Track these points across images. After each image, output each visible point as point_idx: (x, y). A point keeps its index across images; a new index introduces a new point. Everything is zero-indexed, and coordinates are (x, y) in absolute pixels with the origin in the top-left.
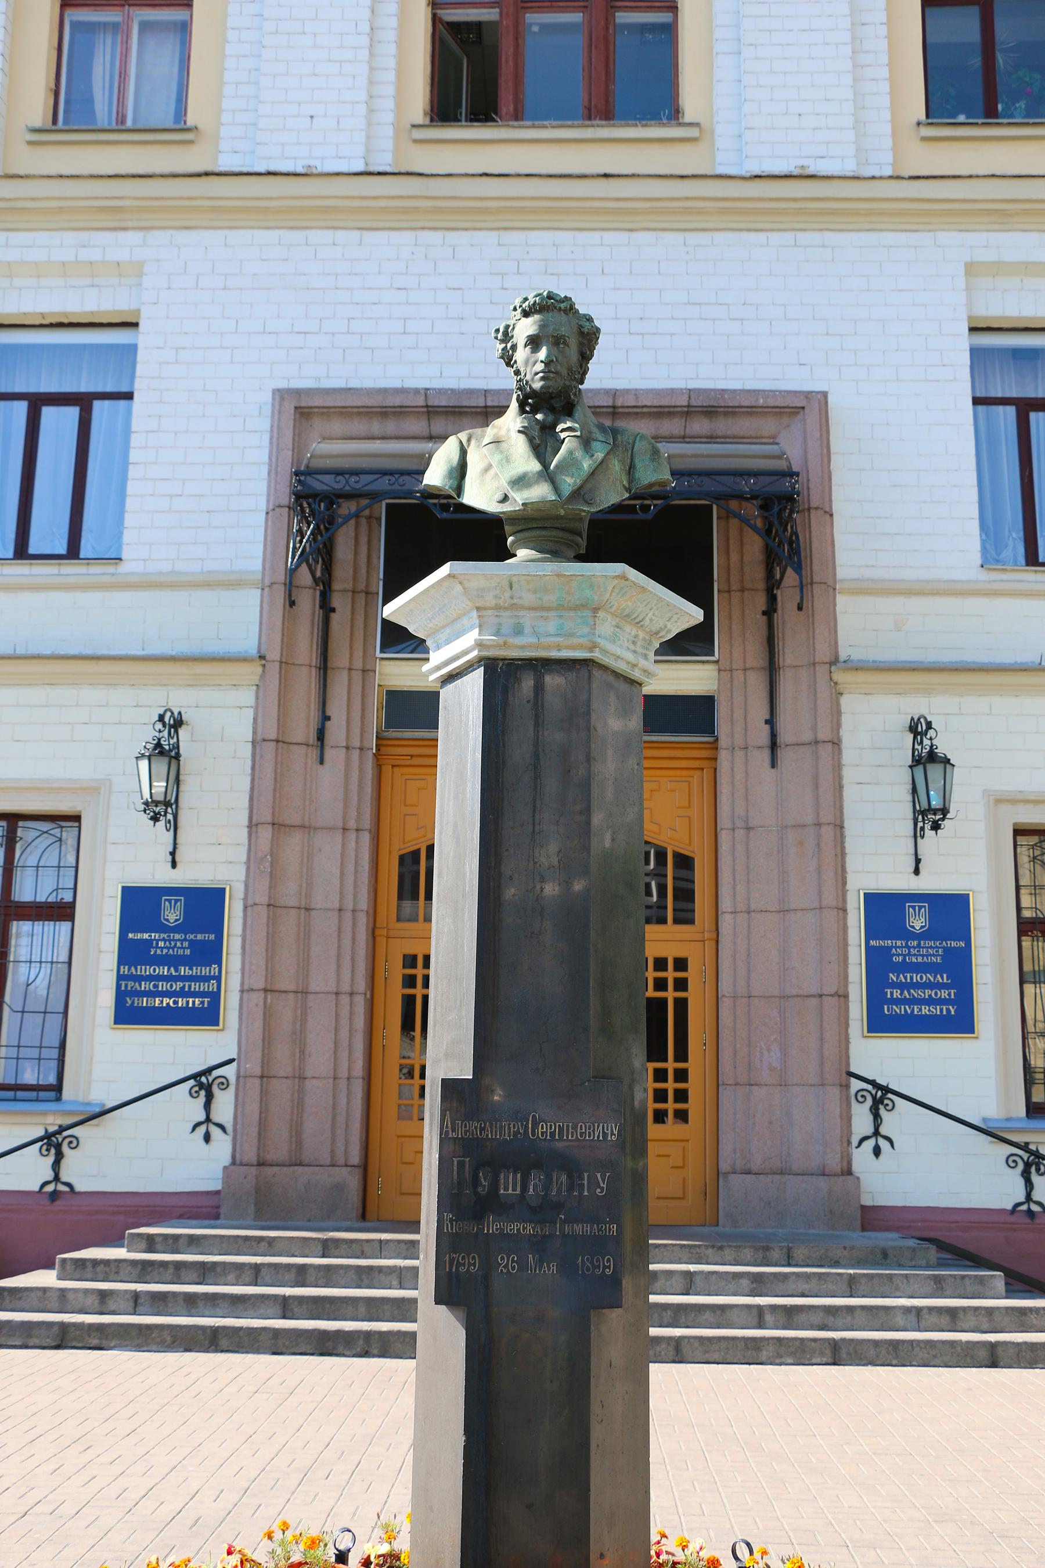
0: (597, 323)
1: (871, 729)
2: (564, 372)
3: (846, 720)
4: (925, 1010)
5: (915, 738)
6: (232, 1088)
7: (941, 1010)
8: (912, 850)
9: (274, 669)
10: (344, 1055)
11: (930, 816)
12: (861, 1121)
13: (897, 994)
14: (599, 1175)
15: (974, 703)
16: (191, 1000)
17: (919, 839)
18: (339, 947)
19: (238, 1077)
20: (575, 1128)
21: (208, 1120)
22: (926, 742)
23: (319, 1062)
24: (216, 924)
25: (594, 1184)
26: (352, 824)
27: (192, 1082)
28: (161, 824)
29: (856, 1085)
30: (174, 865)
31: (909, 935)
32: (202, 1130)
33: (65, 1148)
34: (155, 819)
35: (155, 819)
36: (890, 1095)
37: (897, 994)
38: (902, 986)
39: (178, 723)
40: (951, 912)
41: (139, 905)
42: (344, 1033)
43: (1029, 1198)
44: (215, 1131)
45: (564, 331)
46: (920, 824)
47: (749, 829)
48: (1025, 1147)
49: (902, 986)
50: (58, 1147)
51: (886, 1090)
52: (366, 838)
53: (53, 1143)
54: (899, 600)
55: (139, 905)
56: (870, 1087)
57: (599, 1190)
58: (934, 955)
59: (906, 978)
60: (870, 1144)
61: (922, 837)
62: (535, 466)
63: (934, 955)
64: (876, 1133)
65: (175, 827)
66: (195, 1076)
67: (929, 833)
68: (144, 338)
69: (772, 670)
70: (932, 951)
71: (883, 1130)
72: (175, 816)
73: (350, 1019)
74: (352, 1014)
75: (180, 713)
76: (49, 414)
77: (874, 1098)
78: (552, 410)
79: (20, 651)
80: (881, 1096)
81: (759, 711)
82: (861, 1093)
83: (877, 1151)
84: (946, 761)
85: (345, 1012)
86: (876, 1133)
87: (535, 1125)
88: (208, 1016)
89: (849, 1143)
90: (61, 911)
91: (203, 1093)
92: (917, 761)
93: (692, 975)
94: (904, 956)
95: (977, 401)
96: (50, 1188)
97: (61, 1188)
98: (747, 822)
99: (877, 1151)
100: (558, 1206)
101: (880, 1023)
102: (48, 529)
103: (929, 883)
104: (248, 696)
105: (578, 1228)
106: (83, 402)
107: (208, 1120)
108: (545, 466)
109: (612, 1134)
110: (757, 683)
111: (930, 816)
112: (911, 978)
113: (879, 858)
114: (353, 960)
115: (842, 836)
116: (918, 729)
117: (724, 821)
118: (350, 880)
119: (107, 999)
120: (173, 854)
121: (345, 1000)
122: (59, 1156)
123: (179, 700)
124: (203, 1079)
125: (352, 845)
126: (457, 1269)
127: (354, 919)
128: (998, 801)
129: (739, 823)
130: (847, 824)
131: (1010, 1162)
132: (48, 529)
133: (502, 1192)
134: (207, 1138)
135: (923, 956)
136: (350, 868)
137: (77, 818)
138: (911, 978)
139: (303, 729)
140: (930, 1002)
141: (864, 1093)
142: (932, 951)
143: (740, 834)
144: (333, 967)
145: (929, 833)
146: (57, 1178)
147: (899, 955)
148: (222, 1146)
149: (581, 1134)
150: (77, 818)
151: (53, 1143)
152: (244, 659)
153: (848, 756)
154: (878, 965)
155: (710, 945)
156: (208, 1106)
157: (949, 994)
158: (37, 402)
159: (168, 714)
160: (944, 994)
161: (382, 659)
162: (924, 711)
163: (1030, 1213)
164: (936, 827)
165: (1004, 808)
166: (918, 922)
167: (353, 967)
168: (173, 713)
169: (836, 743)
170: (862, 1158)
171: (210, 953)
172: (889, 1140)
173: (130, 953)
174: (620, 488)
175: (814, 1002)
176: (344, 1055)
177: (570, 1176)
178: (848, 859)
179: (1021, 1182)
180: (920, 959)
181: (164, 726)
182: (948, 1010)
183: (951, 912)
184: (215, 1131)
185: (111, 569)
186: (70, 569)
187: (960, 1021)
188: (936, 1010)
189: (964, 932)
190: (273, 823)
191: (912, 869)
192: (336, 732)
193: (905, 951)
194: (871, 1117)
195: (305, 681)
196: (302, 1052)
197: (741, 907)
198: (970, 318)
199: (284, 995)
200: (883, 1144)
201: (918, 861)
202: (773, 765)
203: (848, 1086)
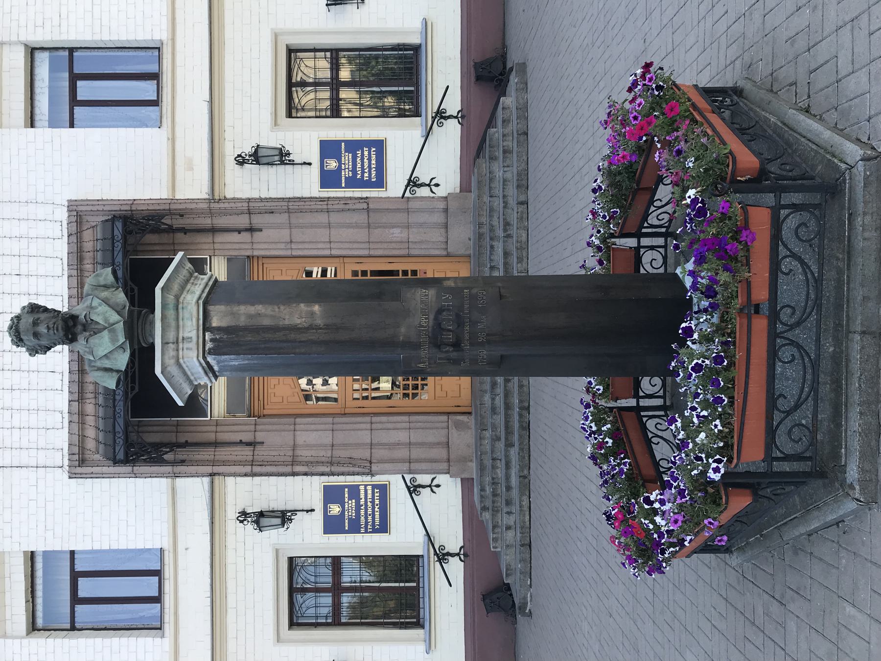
0: (26, 304)
1: (243, 184)
2: (54, 320)
3: (238, 195)
4: (373, 162)
6: (415, 476)
9: (216, 469)
10: (399, 426)
11: (282, 157)
12: (424, 192)
13: (366, 175)
15: (228, 135)
19: (410, 473)
21: (430, 486)
23: (402, 436)
25: (447, 300)
26: (292, 427)
27: (413, 495)
29: (407, 194)
30: (313, 510)
32: (434, 488)
33: (445, 552)
37: (366, 175)
38: (363, 172)
40: (328, 149)
41: (332, 526)
43: (456, 117)
44: (435, 483)
45: (31, 320)
47: (291, 242)
48: (434, 118)
49: (363, 172)
50: (444, 555)
51: (410, 180)
52: (298, 420)
53: (443, 557)
54: (177, 168)
55: (332, 526)
62: (106, 332)
64: (429, 185)
65: (294, 512)
66: (411, 494)
68: (39, 547)
69: (214, 230)
70: (347, 158)
71: (428, 182)
72: (290, 511)
76: (82, 594)
78: (75, 325)
79: (209, 594)
80: (413, 183)
81: (234, 237)
83: (437, 185)
85: (379, 426)
86: (429, 185)
87: (423, 326)
88: (383, 490)
90: (336, 562)
93: (359, 268)
95: (72, 125)
96: (462, 557)
97: (462, 552)
99: (437, 185)
100: (458, 315)
101: (380, 183)
102: (146, 587)
103: (315, 159)
104: (230, 480)
105: (466, 306)
106: (75, 576)
107: (430, 486)
108: (105, 328)
110: (220, 238)
111: (282, 157)
114: (355, 423)
115: (294, 198)
116: (241, 161)
117: (288, 253)
119: (377, 537)
120: (307, 511)
121: (374, 426)
122: (449, 554)
123: (232, 513)
128: (276, 124)
129: (289, 246)
131: (440, 125)
132: (147, 588)
134: (438, 486)
136: (313, 427)
137: (291, 560)
139: (245, 453)
140: (370, 159)
142: (347, 158)
143: (293, 246)
144: (359, 432)
146: (458, 554)
148: (442, 479)
150: (291, 560)
151: (443, 557)
152: (212, 483)
153: (255, 195)
154: (353, 183)
155: (346, 260)
156: (424, 487)
158: (76, 600)
160: (366, 153)
163: (462, 117)
165: (279, 122)
169: (249, 200)
170: (440, 192)
172: (432, 179)
173: (355, 528)
174: (117, 292)
175: (371, 214)
176: (399, 426)
177: (444, 311)
179: (449, 120)
183: (328, 149)
184: (435, 483)
185: (166, 553)
186: (168, 573)
187: (379, 146)
188: (374, 157)
189: (338, 142)
190: (292, 466)
192: (247, 437)
195: (223, 453)
196: (398, 444)
197: (328, 246)
198: (25, 127)
200: (433, 182)
201: (305, 163)
203: (408, 198)
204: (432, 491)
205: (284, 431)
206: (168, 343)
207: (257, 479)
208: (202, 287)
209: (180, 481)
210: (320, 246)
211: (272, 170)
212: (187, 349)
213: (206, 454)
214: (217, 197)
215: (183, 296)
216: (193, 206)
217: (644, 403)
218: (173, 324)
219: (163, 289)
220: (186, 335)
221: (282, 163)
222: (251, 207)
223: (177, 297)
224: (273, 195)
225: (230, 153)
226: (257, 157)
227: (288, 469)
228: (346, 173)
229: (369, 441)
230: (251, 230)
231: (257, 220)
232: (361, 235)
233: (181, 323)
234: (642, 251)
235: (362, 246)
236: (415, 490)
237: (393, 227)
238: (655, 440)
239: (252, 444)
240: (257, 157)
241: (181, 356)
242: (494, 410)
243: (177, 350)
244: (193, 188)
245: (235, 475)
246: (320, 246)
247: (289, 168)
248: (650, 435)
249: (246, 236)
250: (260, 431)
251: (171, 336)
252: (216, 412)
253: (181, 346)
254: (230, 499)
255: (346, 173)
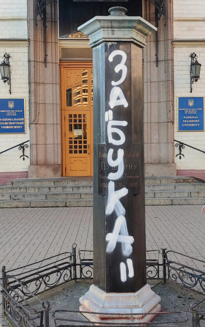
1: (181, 57)
3: (175, 54)
5: (192, 58)
6: (29, 147)
7: (196, 125)
8: (190, 87)
9: (32, 43)
10: (56, 139)
12: (177, 151)
13: (185, 121)
14: (135, 165)
16: (17, 127)
17: (192, 84)
18: (53, 113)
20: (129, 154)
21: (24, 155)
22: (195, 59)
23: (50, 140)
24: (22, 108)
27: (19, 146)
28: (7, 83)
29: (176, 143)
30: (10, 93)
31: (189, 107)
32: (23, 157)
34: (5, 82)
35: (5, 82)
36: (183, 145)
37: (185, 121)
39: (8, 57)
42: (55, 133)
44: (25, 157)
46: (192, 80)
47: (151, 82)
52: (58, 86)
56: (179, 143)
57: (135, 168)
58: (195, 112)
59: (188, 117)
60: (179, 156)
61: (193, 83)
63: (195, 112)
64: (180, 154)
65: (10, 84)
66: (20, 145)
67: (194, 82)
70: (194, 111)
71: (182, 153)
73: (57, 130)
74: (57, 129)
75: (9, 54)
77: (180, 146)
80: (181, 145)
81: (153, 52)
82: (177, 145)
83: (180, 158)
84: (200, 65)
85: (55, 128)
86: (180, 154)
88: (22, 131)
89: (174, 156)
91: (22, 149)
92: (192, 64)
94: (187, 112)
98: (150, 80)
99: (180, 158)
101: (182, 128)
103: (195, 94)
104: (26, 50)
107: (24, 155)
109: (138, 156)
110: (153, 45)
112: (189, 117)
113: (182, 89)
114: (57, 116)
115: (174, 84)
118: (55, 97)
120: (10, 90)
121: (55, 125)
123: (9, 50)
124: (22, 145)
125: (55, 88)
126: (103, 187)
127: (56, 106)
129: (149, 81)
130: (174, 80)
133: (113, 169)
134: (24, 159)
135: (192, 112)
138: (189, 117)
141: (178, 145)
143: (149, 83)
144: (52, 118)
145: (194, 82)
147: (186, 112)
148: (28, 161)
149: (130, 156)
153: (175, 63)
157: (198, 121)
159: (6, 55)
160: (197, 121)
161: (59, 40)
162: (194, 52)
164: (196, 81)
166: (191, 104)
167: (57, 118)
168: (7, 54)
169: (172, 60)
170: (177, 159)
171: (22, 115)
172: (183, 155)
175: (166, 124)
176: (56, 139)
178: (175, 89)
180: (191, 113)
181: (5, 58)
182: (198, 125)
184: (25, 157)
190: (34, 83)
191: (190, 91)
192: (49, 59)
193: (188, 111)
194: (179, 150)
195: (41, 46)
196: (46, 138)
199: (40, 125)
200: (182, 156)
201: (191, 89)
202: (157, 66)
203: (174, 143)
204: (21, 156)
205: (53, 78)
206: (111, 23)
207: (27, 64)
208: (140, 40)
209: (25, 23)
210: (149, 97)
211: (188, 72)
212: (108, 33)
213: (40, 37)
214: (174, 43)
215: (135, 31)
216: (169, 29)
217: (78, 267)
218: (121, 25)
219: (140, 20)
220: (115, 32)
221: (192, 78)
222: (169, 61)
223: (134, 28)
224: (176, 73)
225: (197, 50)
226: (195, 65)
227: (32, 80)
228: (186, 111)
229: (47, 123)
230: (157, 61)
231: (162, 65)
232: (155, 119)
233: (122, 29)
234: (156, 267)
235: (149, 119)
236: (21, 147)
237: (159, 135)
238: (59, 274)
239: (45, 62)
240: (195, 65)
241: (105, 29)
242: (64, 187)
243: (108, 28)
244: (179, 31)
245: (29, 53)
246: (149, 97)
247: (189, 81)
248: (61, 271)
249: (154, 58)
250: (52, 66)
251: (115, 25)
252: (62, 42)
253: (110, 29)
254: (16, 49)
255: (186, 111)
